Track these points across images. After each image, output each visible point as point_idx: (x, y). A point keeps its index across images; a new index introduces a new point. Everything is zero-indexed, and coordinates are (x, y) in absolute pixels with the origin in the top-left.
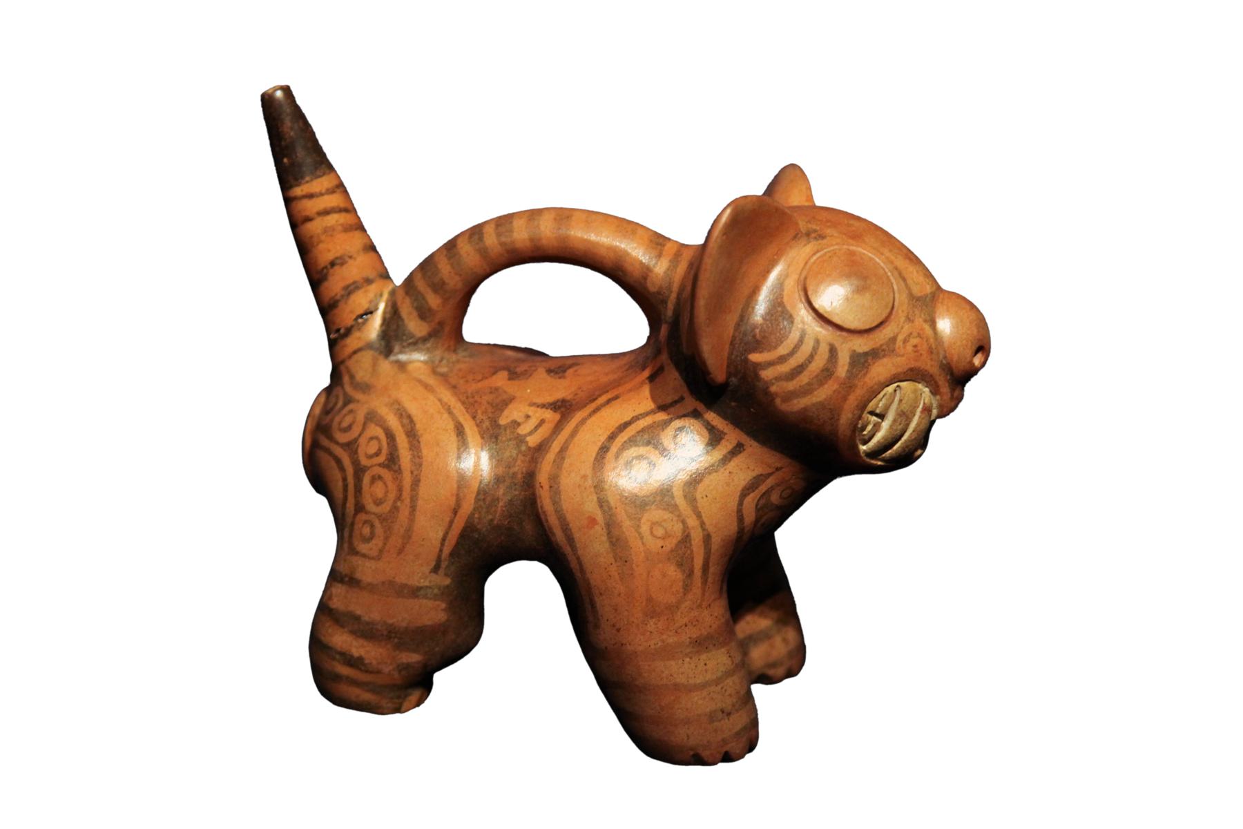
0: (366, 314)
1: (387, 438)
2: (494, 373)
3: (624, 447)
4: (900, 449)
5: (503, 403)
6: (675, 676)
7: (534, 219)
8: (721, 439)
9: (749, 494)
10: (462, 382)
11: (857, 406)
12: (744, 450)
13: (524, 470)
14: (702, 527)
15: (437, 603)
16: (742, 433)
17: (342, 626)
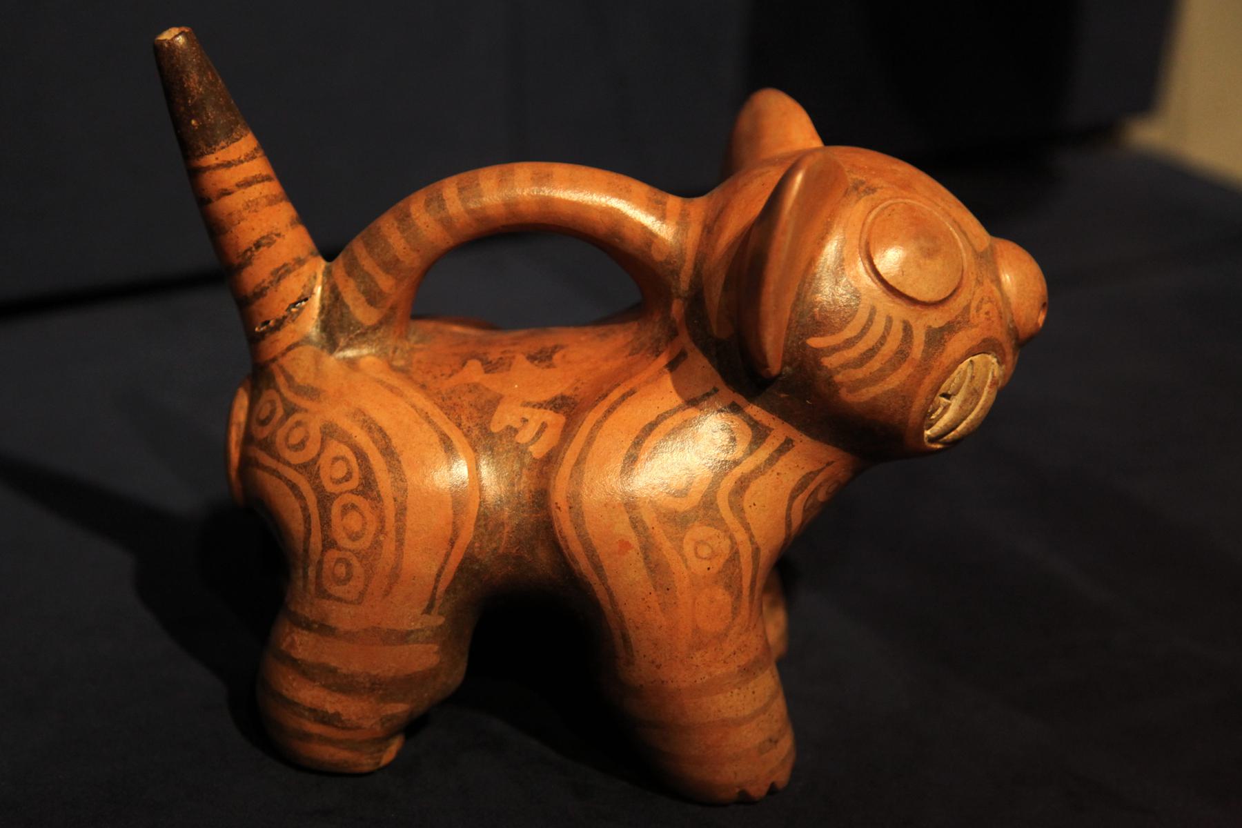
0: (300, 301)
1: (357, 458)
2: (464, 365)
4: (965, 430)
5: (489, 405)
6: (723, 711)
7: (505, 180)
8: (767, 435)
9: (798, 496)
10: (429, 378)
11: (931, 390)
12: (793, 446)
13: (532, 488)
14: (751, 540)
15: (430, 645)
16: (792, 427)
17: (313, 680)
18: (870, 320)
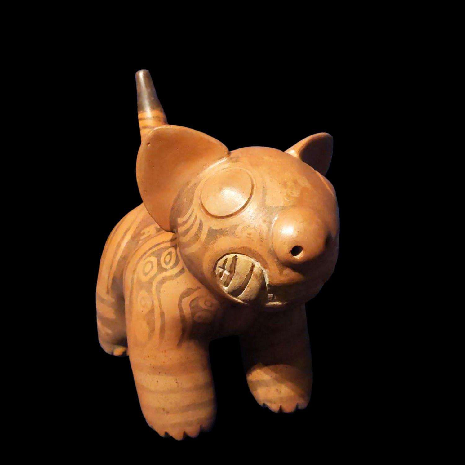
3: (150, 256)
9: (185, 297)
14: (160, 307)
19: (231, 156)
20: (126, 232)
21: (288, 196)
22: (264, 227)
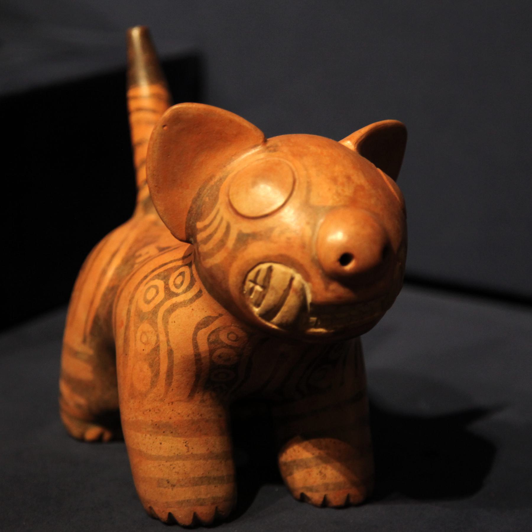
3: (153, 279)
9: (202, 329)
12: (202, 295)
18: (215, 217)
19: (268, 144)
20: (114, 255)
21: (338, 194)
22: (308, 231)
